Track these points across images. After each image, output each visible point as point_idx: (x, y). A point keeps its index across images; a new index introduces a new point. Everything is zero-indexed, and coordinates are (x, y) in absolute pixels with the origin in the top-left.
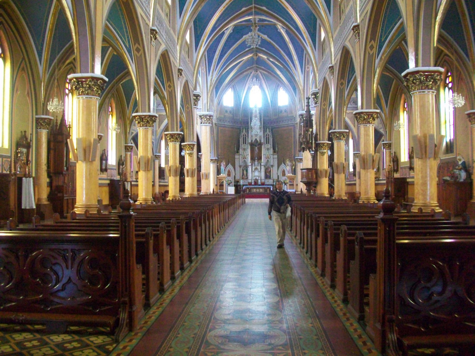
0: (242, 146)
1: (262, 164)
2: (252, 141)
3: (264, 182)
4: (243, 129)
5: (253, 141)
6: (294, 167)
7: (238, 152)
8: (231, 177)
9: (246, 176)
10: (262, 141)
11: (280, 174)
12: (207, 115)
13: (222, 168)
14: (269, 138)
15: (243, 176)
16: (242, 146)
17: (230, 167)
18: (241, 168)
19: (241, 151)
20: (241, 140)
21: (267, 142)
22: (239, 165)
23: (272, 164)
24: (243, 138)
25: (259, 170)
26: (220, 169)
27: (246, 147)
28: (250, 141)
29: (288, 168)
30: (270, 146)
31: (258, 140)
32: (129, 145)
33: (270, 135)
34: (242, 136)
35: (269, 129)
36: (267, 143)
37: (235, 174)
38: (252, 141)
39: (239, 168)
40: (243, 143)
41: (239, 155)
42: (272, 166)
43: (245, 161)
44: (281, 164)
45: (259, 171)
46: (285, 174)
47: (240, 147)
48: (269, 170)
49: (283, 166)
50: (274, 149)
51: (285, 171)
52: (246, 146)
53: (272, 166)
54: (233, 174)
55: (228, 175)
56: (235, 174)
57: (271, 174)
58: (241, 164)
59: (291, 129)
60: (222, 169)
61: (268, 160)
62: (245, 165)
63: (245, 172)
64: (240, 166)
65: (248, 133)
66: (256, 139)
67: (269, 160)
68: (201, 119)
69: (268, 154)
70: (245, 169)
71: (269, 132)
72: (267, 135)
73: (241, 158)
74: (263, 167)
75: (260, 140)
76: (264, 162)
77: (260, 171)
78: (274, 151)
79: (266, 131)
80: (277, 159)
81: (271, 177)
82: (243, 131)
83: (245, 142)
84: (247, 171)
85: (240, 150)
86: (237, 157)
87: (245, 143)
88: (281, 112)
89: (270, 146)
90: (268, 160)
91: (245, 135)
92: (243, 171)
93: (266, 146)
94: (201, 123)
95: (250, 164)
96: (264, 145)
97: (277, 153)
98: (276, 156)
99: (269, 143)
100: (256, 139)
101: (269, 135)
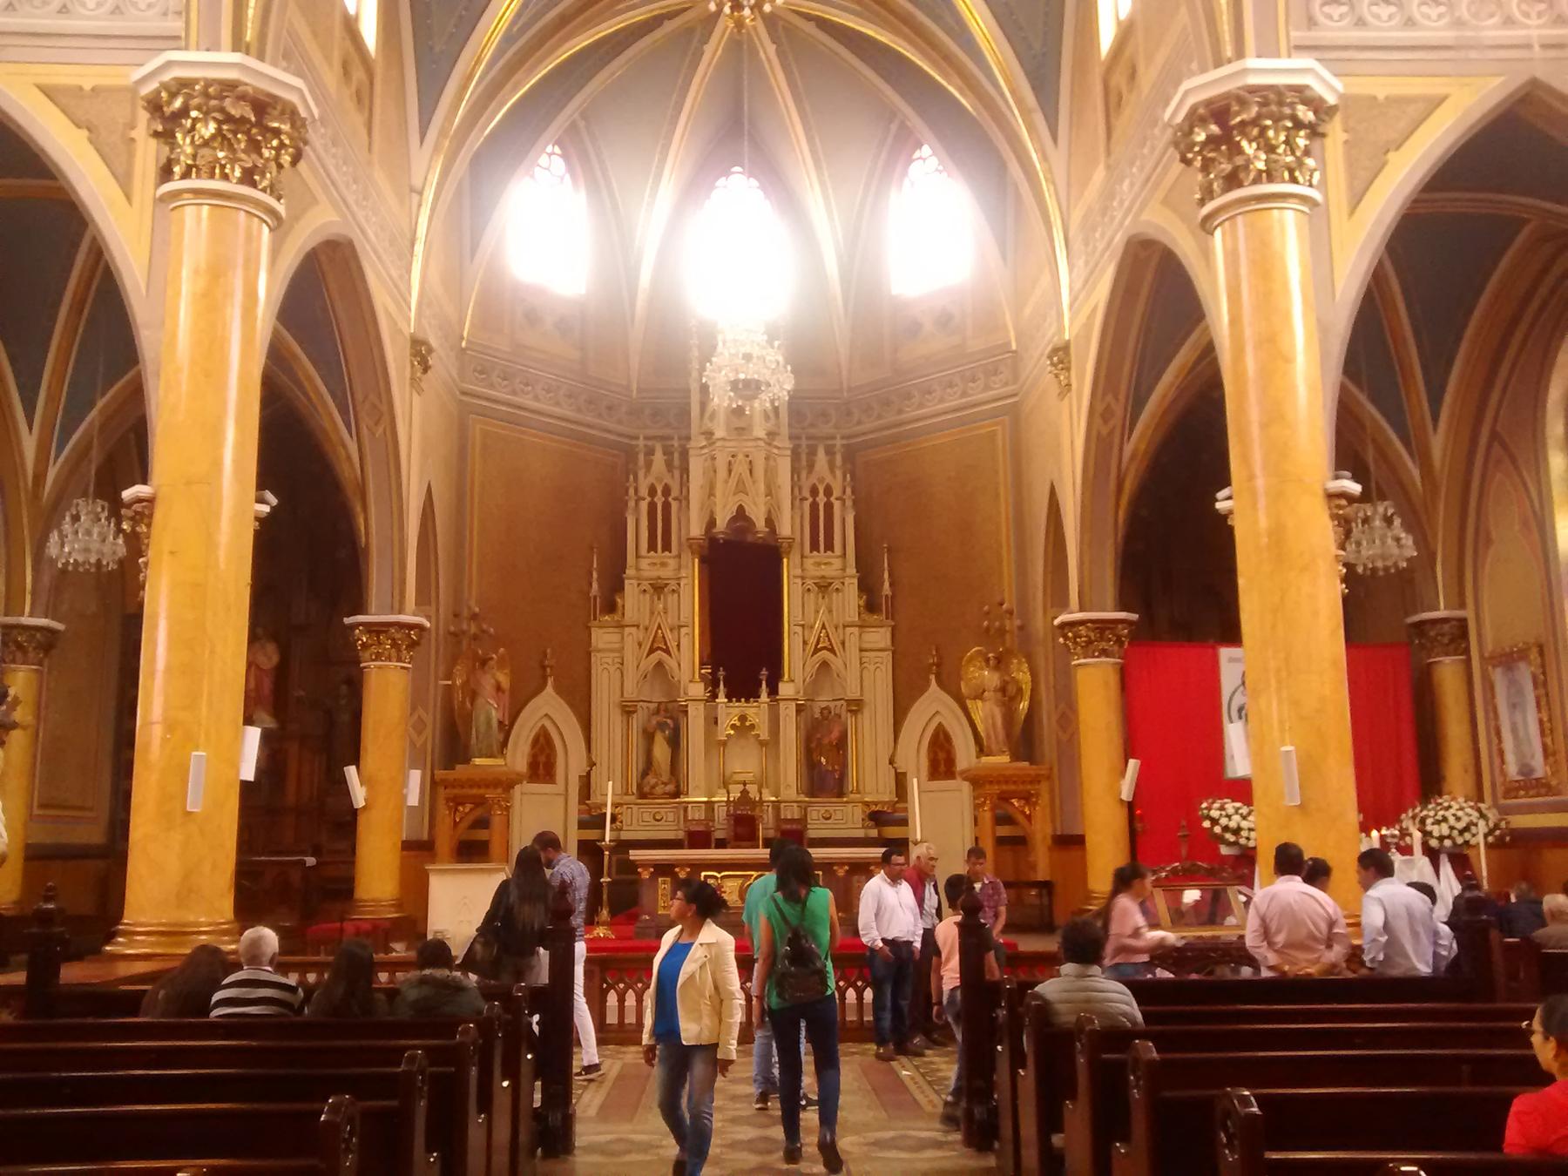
0: (644, 564)
1: (785, 689)
2: (712, 523)
3: (803, 820)
4: (650, 452)
5: (721, 524)
6: (1024, 706)
7: (611, 607)
8: (559, 786)
9: (665, 777)
10: (785, 529)
11: (914, 758)
12: (230, 86)
13: (490, 710)
14: (829, 507)
15: (651, 780)
16: (642, 565)
17: (548, 708)
18: (637, 722)
19: (633, 599)
20: (636, 528)
21: (821, 537)
22: (616, 698)
23: (853, 692)
24: (652, 508)
25: (765, 735)
26: (468, 718)
27: (666, 573)
28: (696, 530)
29: (986, 712)
30: (839, 565)
31: (758, 517)
32: (26, 620)
33: (837, 492)
34: (644, 492)
35: (830, 452)
36: (814, 546)
37: (592, 764)
38: (712, 523)
39: (617, 718)
40: (652, 547)
41: (621, 626)
42: (856, 706)
43: (660, 664)
44: (923, 688)
45: (762, 744)
46: (950, 761)
47: (630, 572)
48: (835, 734)
49: (933, 706)
50: (867, 587)
51: (948, 738)
52: (672, 563)
53: (856, 706)
54: (570, 762)
55: (534, 765)
56: (592, 764)
57: (844, 765)
58: (631, 692)
59: (992, 435)
60: (480, 719)
61: (825, 665)
62: (658, 697)
63: (661, 751)
64: (628, 710)
65: (685, 470)
66: (741, 509)
67: (836, 662)
68: (166, 136)
69: (822, 615)
70: (661, 726)
71: (832, 470)
72: (814, 491)
73: (630, 644)
74: (788, 712)
75: (769, 522)
76: (799, 680)
77: (771, 745)
78: (871, 607)
79: (811, 466)
80: (887, 657)
81: (852, 782)
82: (649, 465)
83: (661, 539)
84: (675, 742)
85: (630, 586)
86: (602, 638)
87: (667, 547)
88: (914, 329)
89: (837, 563)
90: (825, 665)
91: (667, 491)
92: (649, 737)
93: (809, 563)
94: (166, 173)
95: (698, 690)
96: (795, 556)
97: (891, 615)
98: (880, 637)
99: (829, 546)
100: (741, 509)
101: (828, 491)
